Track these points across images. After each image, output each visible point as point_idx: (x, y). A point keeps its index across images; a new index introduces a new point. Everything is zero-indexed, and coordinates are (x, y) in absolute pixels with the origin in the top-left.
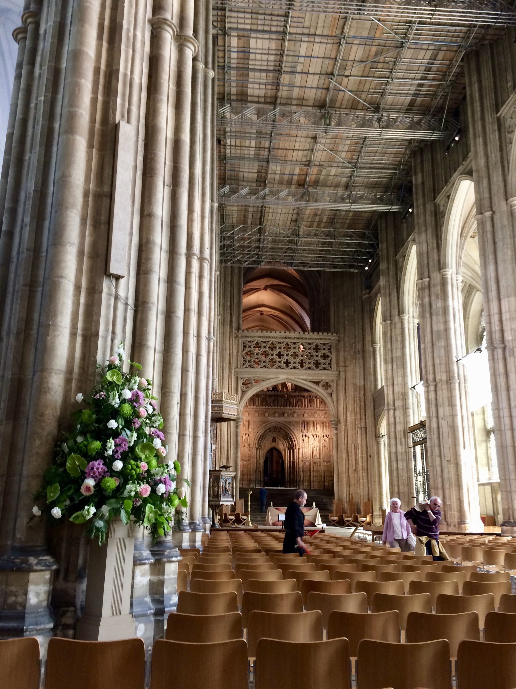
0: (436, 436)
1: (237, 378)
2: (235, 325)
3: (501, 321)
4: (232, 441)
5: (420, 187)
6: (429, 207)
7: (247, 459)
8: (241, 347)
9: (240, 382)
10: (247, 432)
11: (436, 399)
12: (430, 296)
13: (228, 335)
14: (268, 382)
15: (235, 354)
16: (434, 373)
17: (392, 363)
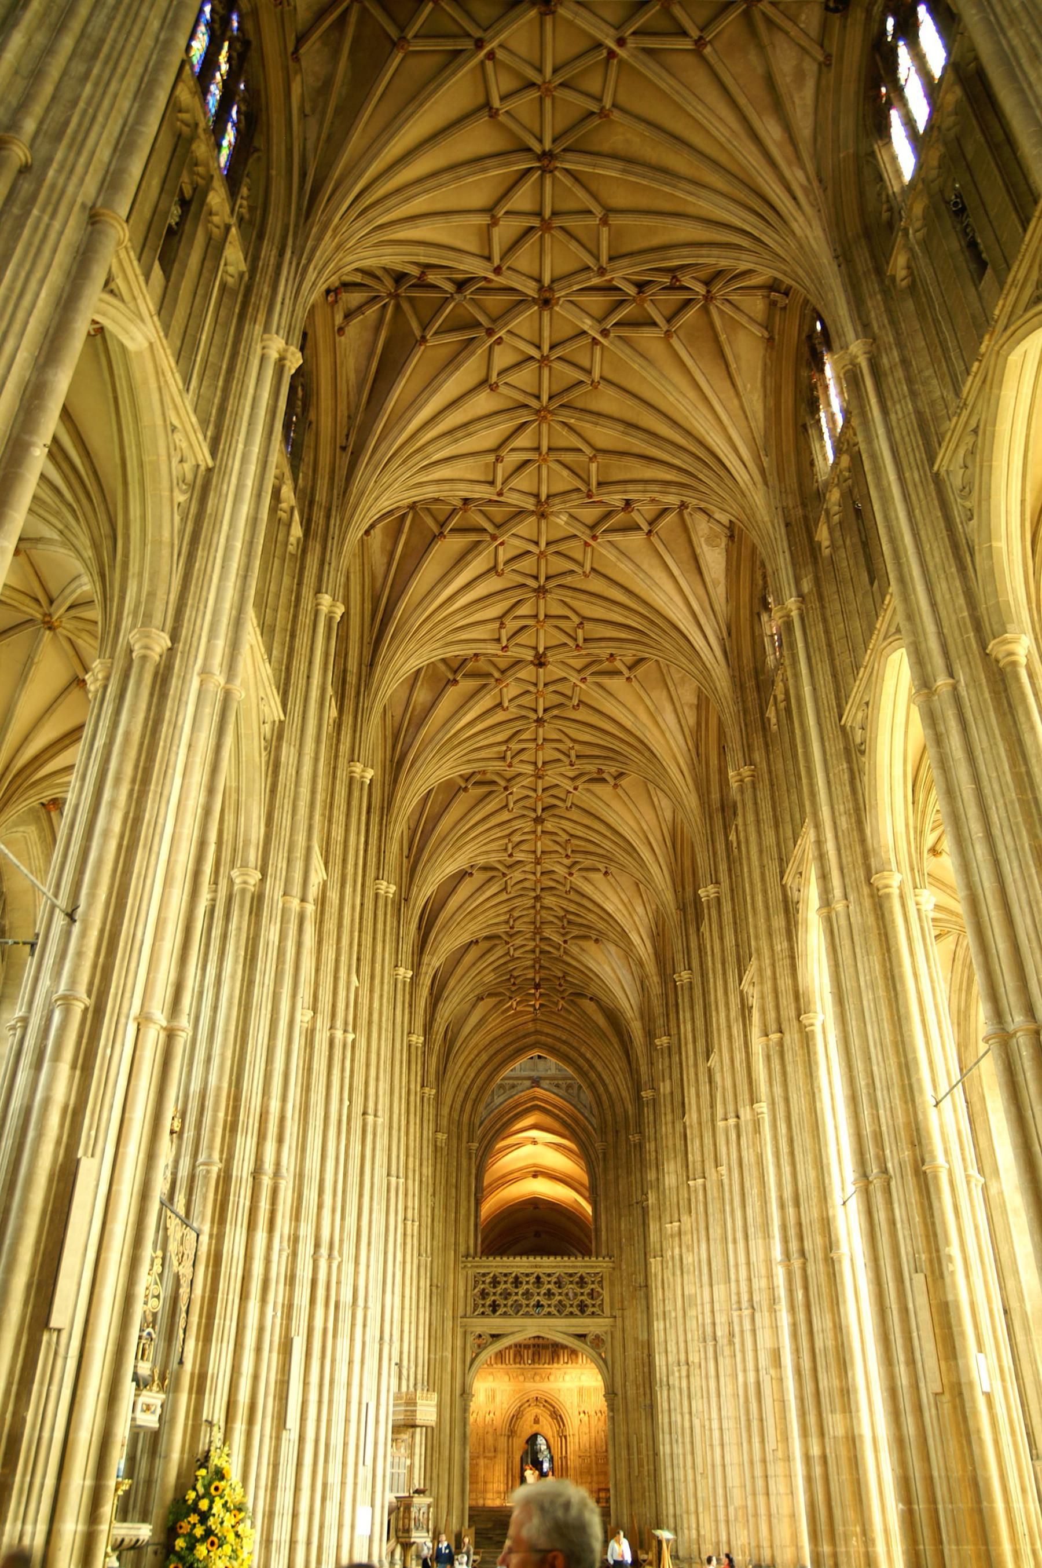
0: (688, 1439)
1: (465, 1333)
2: (462, 1249)
3: (713, 1312)
4: (457, 1434)
5: (668, 1098)
6: (679, 1127)
7: (492, 1454)
8: (471, 1283)
9: (470, 1339)
10: (491, 1408)
11: (689, 1388)
12: (680, 1247)
13: (452, 1265)
14: (511, 1337)
15: (462, 1293)
16: (687, 1353)
17: (665, 1319)
